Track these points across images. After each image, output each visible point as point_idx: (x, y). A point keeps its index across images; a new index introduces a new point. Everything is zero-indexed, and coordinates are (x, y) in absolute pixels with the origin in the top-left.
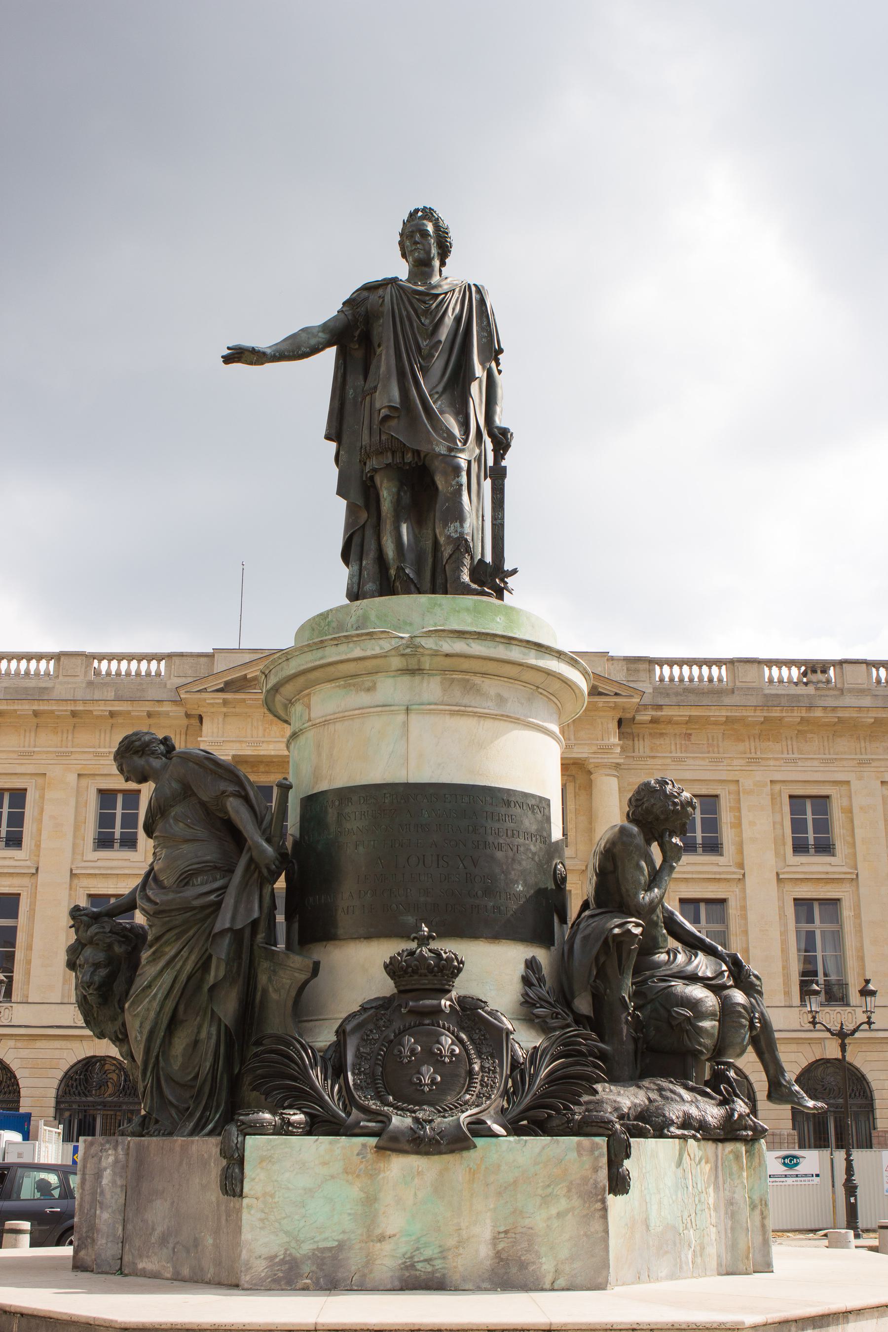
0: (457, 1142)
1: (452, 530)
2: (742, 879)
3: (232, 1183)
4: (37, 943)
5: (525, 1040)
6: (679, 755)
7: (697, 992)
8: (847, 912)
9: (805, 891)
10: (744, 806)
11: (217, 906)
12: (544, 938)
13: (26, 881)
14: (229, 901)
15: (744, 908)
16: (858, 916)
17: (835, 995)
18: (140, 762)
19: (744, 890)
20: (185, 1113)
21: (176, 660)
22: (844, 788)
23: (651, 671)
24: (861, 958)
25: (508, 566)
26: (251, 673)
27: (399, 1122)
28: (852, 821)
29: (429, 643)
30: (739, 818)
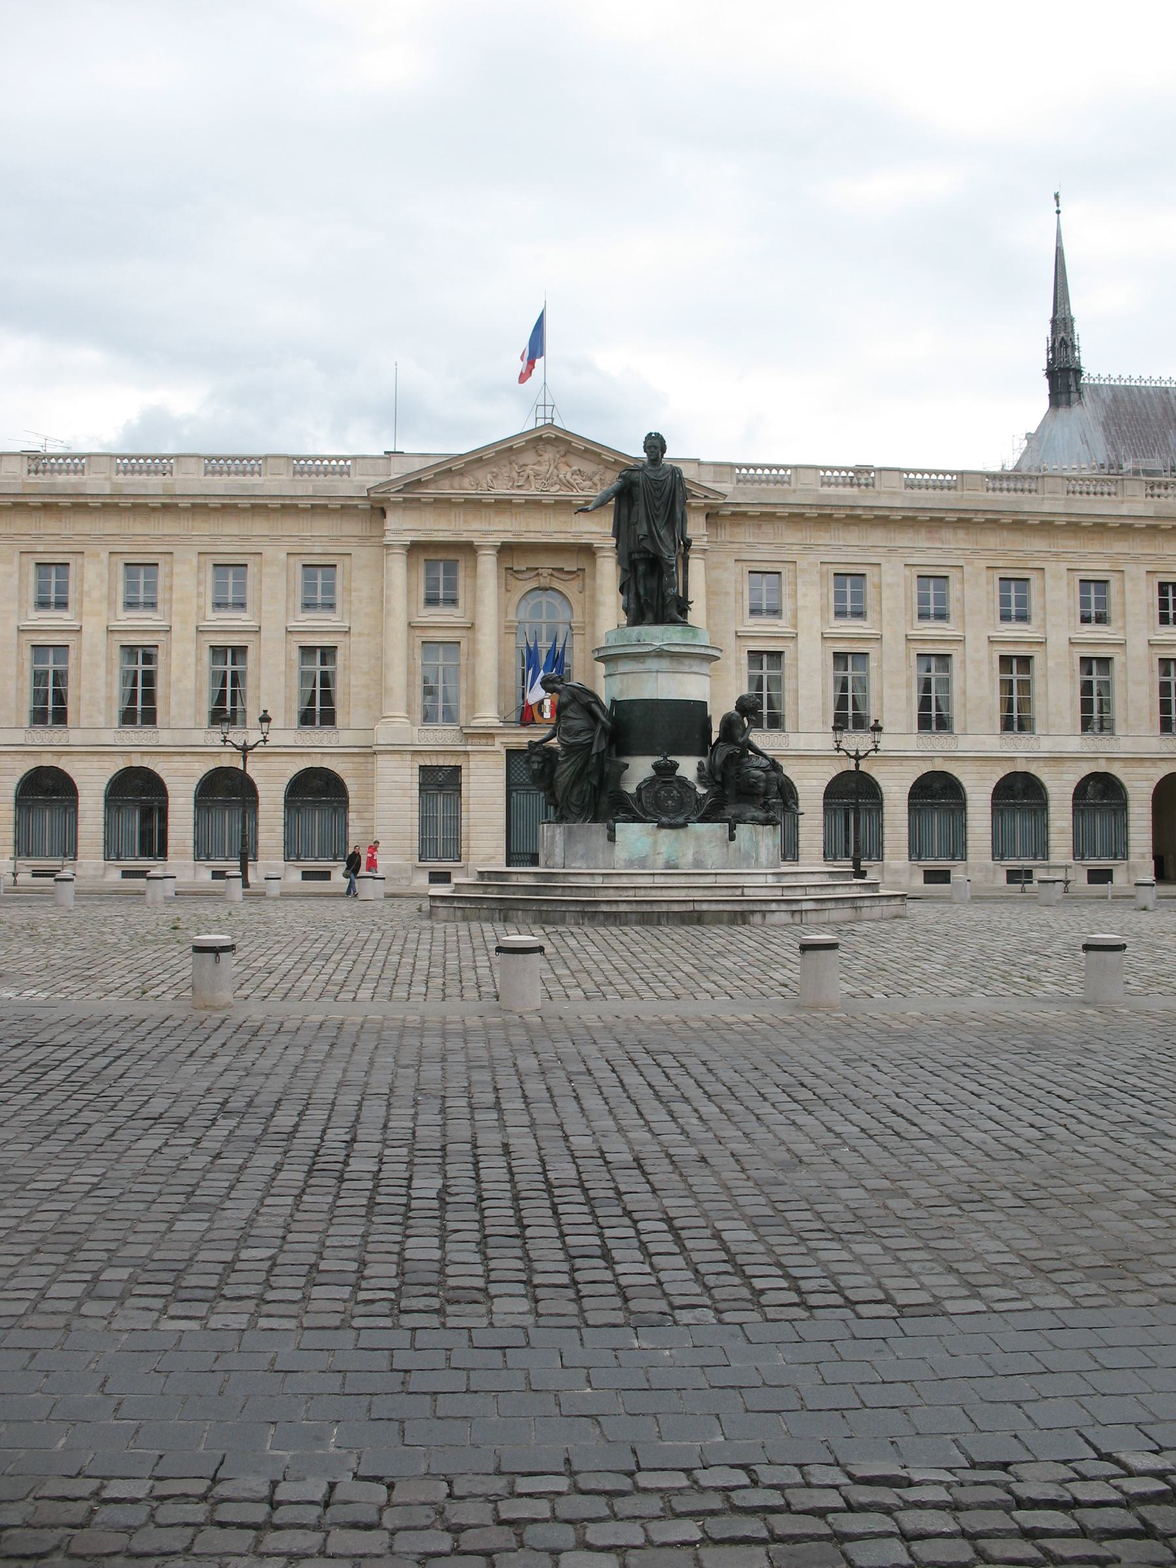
0: (684, 826)
1: (671, 591)
2: (794, 638)
3: (612, 838)
4: (264, 684)
5: (701, 790)
6: (751, 540)
7: (759, 773)
8: (872, 664)
9: (842, 647)
10: (799, 581)
11: (591, 744)
12: (703, 753)
13: (251, 637)
14: (595, 743)
15: (796, 659)
16: (880, 666)
17: (860, 723)
18: (550, 686)
19: (796, 645)
20: (579, 815)
21: (360, 461)
22: (876, 569)
23: (733, 473)
24: (881, 698)
25: (690, 600)
26: (425, 477)
27: (664, 819)
28: (881, 594)
29: (666, 648)
30: (796, 591)
